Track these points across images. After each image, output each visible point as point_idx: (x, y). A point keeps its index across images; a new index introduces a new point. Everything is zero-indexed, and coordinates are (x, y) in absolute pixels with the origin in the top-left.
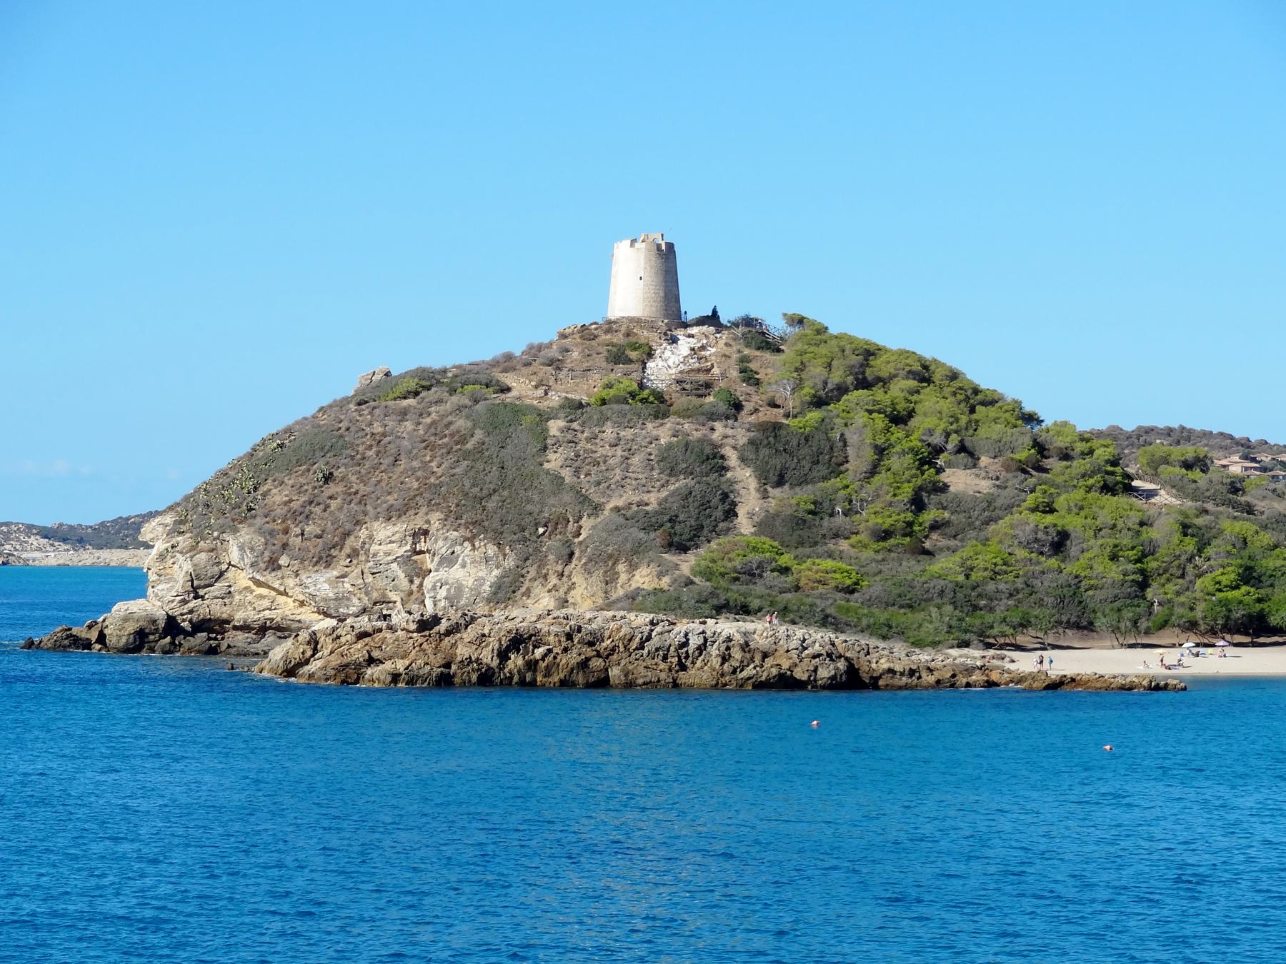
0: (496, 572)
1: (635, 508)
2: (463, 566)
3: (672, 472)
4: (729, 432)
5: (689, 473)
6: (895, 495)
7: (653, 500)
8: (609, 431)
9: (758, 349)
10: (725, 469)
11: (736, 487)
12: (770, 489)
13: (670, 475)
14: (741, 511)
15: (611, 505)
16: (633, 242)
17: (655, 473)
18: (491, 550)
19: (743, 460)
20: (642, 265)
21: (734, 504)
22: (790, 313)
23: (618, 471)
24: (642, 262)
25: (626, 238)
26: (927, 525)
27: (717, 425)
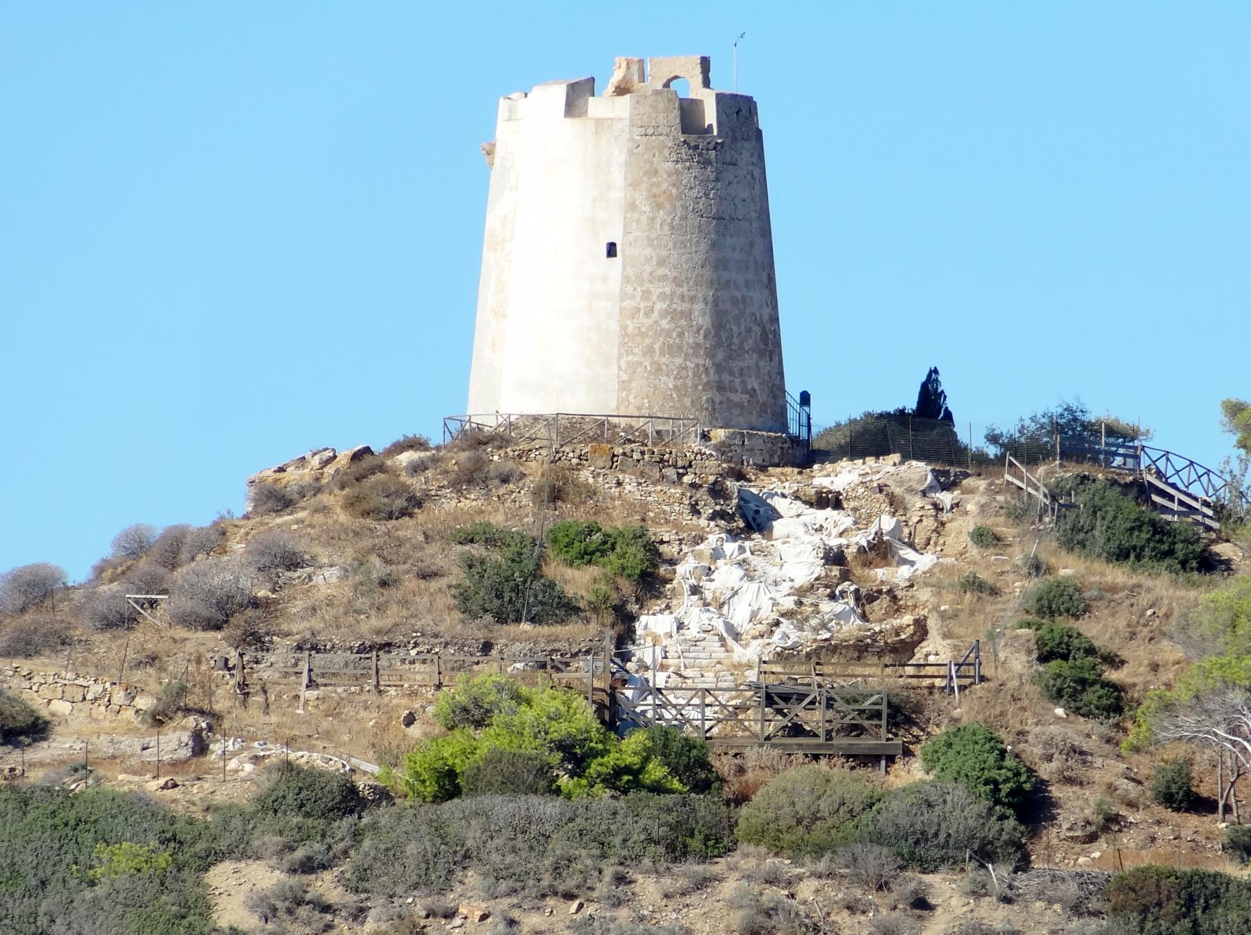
20: (618, 194)
24: (618, 177)
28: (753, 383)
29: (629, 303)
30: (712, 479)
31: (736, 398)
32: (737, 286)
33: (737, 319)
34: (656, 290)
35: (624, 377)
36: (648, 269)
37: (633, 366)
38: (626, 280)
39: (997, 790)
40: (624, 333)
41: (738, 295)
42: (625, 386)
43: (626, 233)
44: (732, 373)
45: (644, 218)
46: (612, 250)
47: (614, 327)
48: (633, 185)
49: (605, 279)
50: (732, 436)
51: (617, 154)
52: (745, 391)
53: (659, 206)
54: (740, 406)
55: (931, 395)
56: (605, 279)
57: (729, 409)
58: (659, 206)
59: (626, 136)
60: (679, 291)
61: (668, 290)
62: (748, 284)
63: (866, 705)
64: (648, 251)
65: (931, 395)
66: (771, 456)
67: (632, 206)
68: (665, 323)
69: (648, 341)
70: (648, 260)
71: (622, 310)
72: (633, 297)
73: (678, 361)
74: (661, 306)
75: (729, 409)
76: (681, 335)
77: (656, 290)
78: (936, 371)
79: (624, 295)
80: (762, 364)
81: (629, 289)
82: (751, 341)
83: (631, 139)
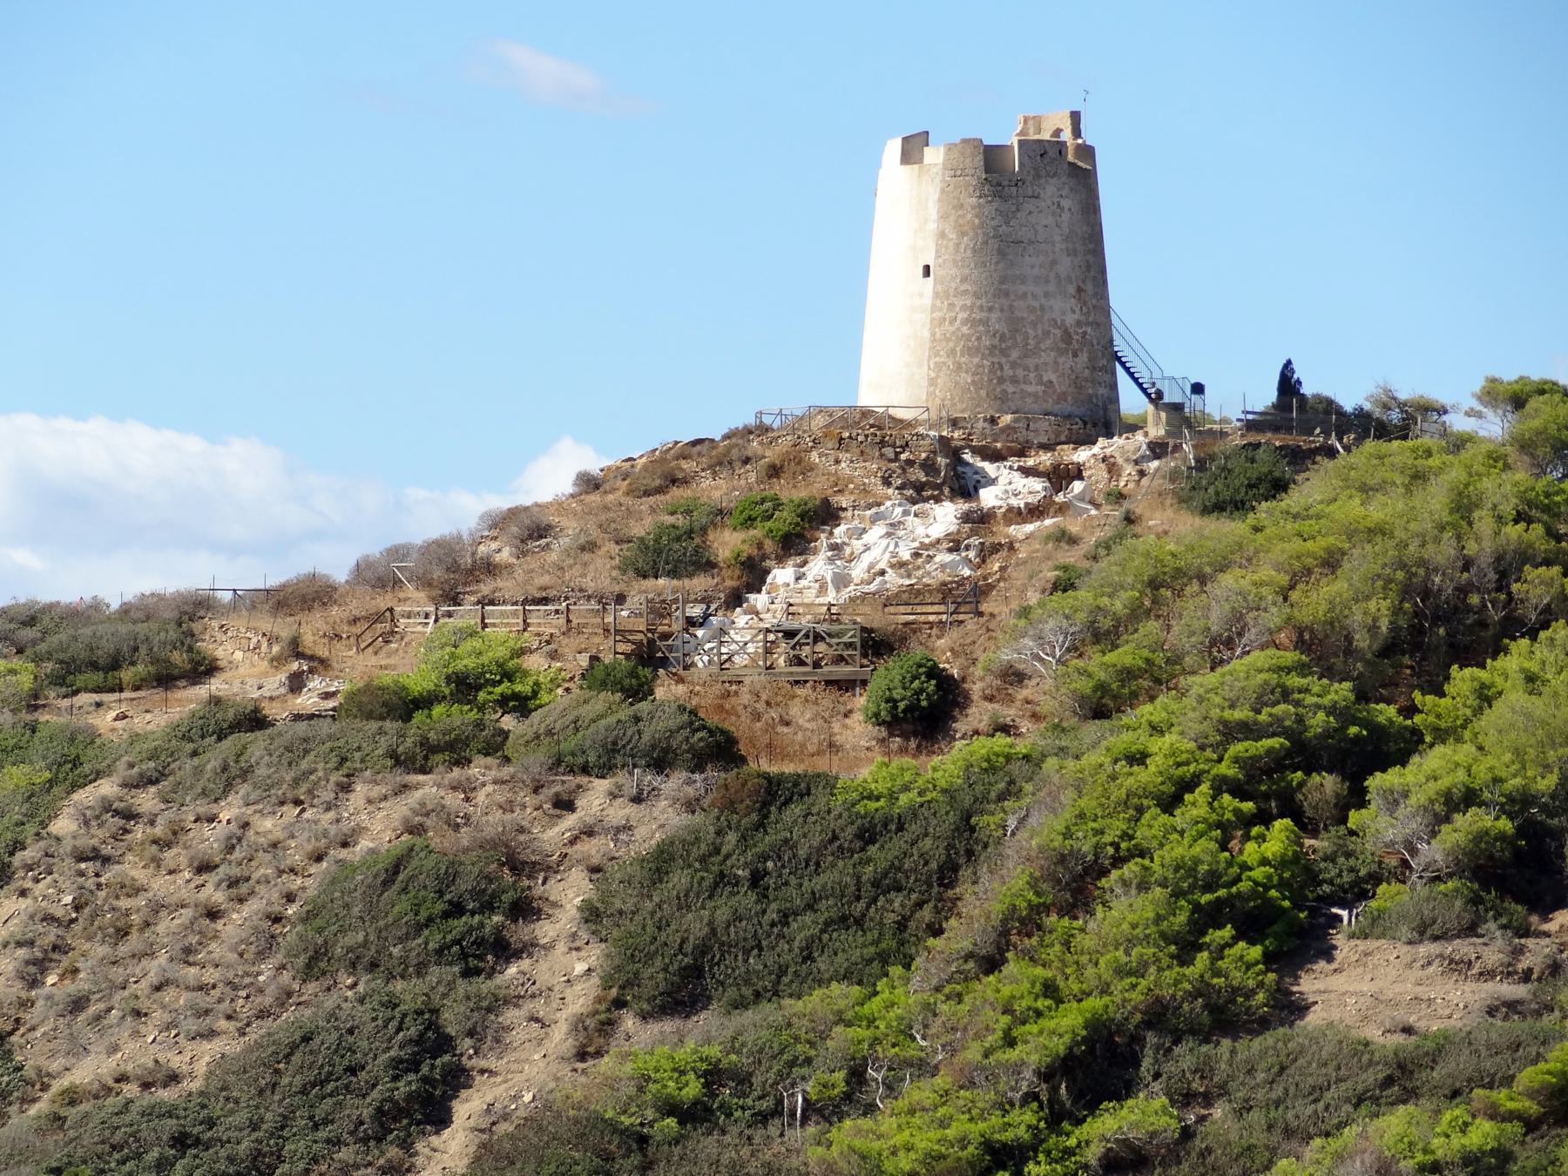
1: (131, 1090)
3: (316, 964)
4: (620, 812)
5: (366, 962)
6: (1010, 1042)
7: (199, 1061)
8: (224, 816)
9: (1206, 511)
10: (527, 949)
11: (511, 1015)
12: (629, 1022)
14: (467, 1108)
15: (65, 1082)
16: (913, 149)
17: (266, 970)
19: (592, 915)
20: (932, 226)
21: (458, 1078)
22: (1509, 374)
23: (162, 958)
24: (933, 211)
25: (892, 137)
26: (1093, 1154)
27: (595, 798)
28: (1050, 376)
29: (938, 314)
30: (924, 455)
31: (1030, 389)
32: (1034, 297)
33: (1034, 325)
34: (959, 302)
35: (933, 375)
36: (953, 285)
37: (939, 366)
38: (936, 295)
39: (896, 707)
40: (934, 340)
41: (1036, 304)
42: (932, 382)
43: (938, 257)
44: (1026, 369)
45: (951, 244)
46: (927, 271)
47: (927, 334)
48: (943, 217)
49: (921, 295)
50: (1016, 421)
51: (932, 192)
52: (1040, 382)
53: (963, 234)
54: (1035, 395)
55: (1288, 384)
56: (921, 295)
57: (1022, 398)
58: (963, 234)
59: (938, 180)
60: (979, 303)
61: (968, 303)
62: (1046, 295)
63: (846, 639)
64: (953, 271)
65: (1288, 384)
66: (1057, 436)
67: (942, 235)
68: (965, 330)
69: (951, 344)
70: (953, 278)
71: (932, 319)
72: (940, 310)
73: (976, 360)
74: (962, 315)
75: (1022, 398)
76: (979, 339)
77: (959, 302)
78: (1289, 362)
79: (934, 308)
80: (1061, 360)
81: (938, 303)
82: (1048, 342)
83: (943, 181)
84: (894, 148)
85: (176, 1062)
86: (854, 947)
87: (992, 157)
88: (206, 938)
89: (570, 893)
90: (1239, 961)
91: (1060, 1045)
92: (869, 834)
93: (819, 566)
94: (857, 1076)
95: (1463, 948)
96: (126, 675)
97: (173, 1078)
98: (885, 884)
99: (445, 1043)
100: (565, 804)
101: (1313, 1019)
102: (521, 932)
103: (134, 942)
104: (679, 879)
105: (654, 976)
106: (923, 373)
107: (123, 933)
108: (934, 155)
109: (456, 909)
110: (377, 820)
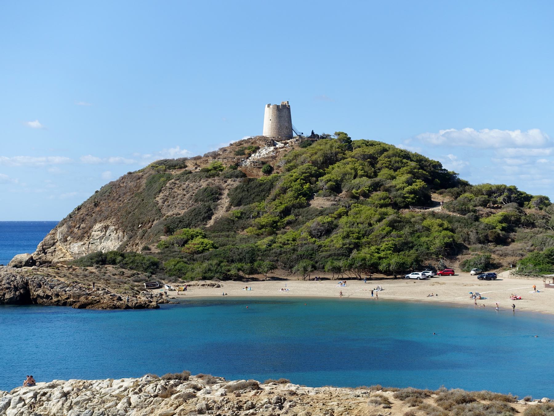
0: (120, 243)
1: (175, 216)
2: (111, 241)
3: (196, 201)
4: (232, 183)
6: (276, 209)
7: (182, 212)
10: (221, 199)
11: (219, 206)
12: (232, 207)
13: (195, 202)
14: (213, 217)
18: (121, 234)
19: (228, 195)
21: (212, 214)
22: (338, 131)
26: (285, 222)
27: (229, 181)
51: (271, 111)
55: (313, 133)
65: (313, 133)
84: (267, 106)
85: (180, 212)
86: (258, 198)
87: (278, 106)
88: (184, 198)
89: (226, 192)
90: (303, 199)
91: (282, 209)
92: (261, 185)
93: (257, 154)
94: (258, 213)
95: (329, 198)
96: (176, 167)
97: (180, 214)
98: (262, 191)
99: (211, 210)
100: (226, 182)
101: (311, 206)
102: (220, 197)
103: (176, 198)
104: (239, 190)
105: (235, 202)
106: (270, 132)
107: (174, 197)
108: (271, 106)
109: (213, 194)
110: (204, 184)
